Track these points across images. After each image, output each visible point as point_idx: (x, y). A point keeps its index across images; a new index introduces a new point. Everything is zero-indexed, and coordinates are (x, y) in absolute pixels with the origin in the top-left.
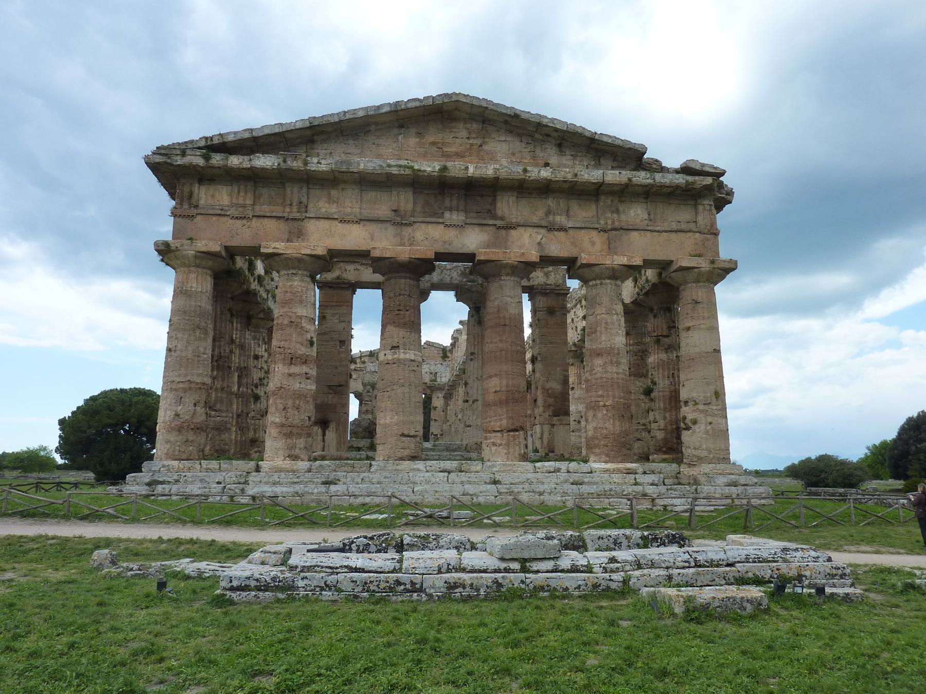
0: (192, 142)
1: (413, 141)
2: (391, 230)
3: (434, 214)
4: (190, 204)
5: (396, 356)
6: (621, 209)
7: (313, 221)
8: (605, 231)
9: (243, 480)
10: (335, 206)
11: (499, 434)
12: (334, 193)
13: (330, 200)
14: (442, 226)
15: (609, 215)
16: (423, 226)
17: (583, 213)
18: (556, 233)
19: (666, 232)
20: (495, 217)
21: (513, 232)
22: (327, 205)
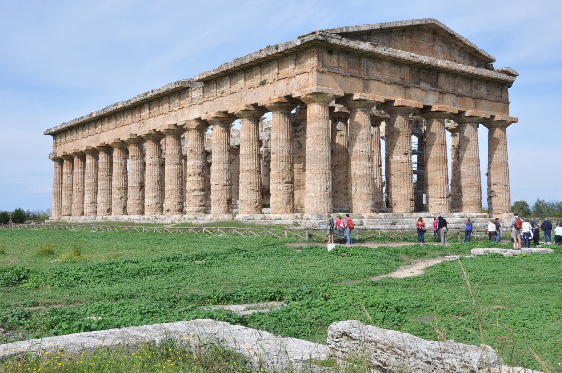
0: (334, 29)
1: (408, 40)
2: (403, 90)
3: (416, 83)
7: (373, 81)
8: (474, 99)
12: (379, 65)
13: (377, 70)
14: (420, 90)
15: (476, 91)
16: (414, 88)
17: (464, 89)
20: (437, 87)
21: (445, 95)
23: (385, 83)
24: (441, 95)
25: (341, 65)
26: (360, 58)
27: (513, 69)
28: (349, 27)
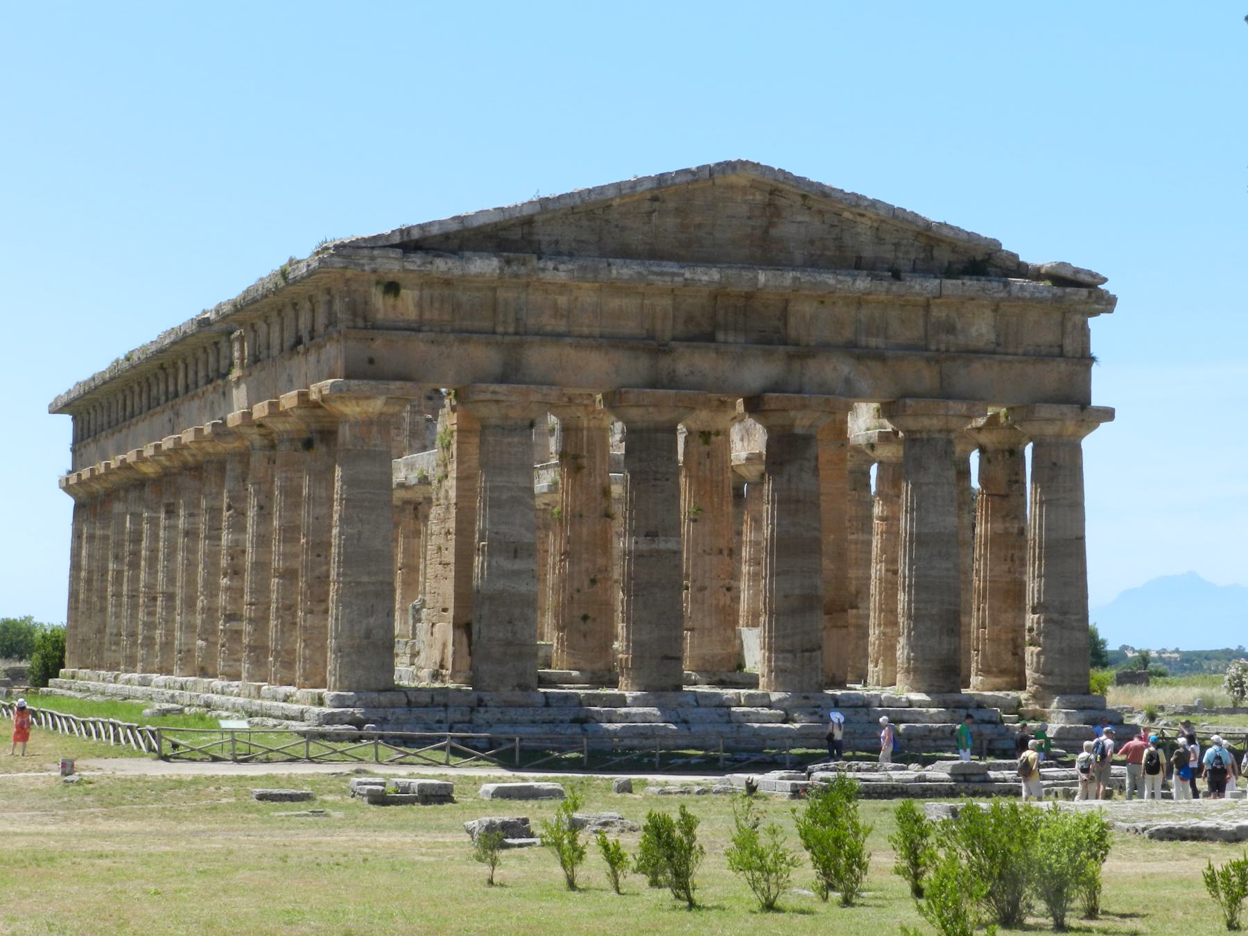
4: (365, 319)
5: (654, 546)
6: (959, 326)
9: (467, 718)
10: (563, 322)
11: (789, 656)
15: (943, 337)
18: (869, 363)
19: (1020, 362)
22: (553, 321)
23: (577, 346)
24: (797, 365)
25: (427, 316)
26: (494, 289)
27: (1081, 260)
28: (431, 224)
